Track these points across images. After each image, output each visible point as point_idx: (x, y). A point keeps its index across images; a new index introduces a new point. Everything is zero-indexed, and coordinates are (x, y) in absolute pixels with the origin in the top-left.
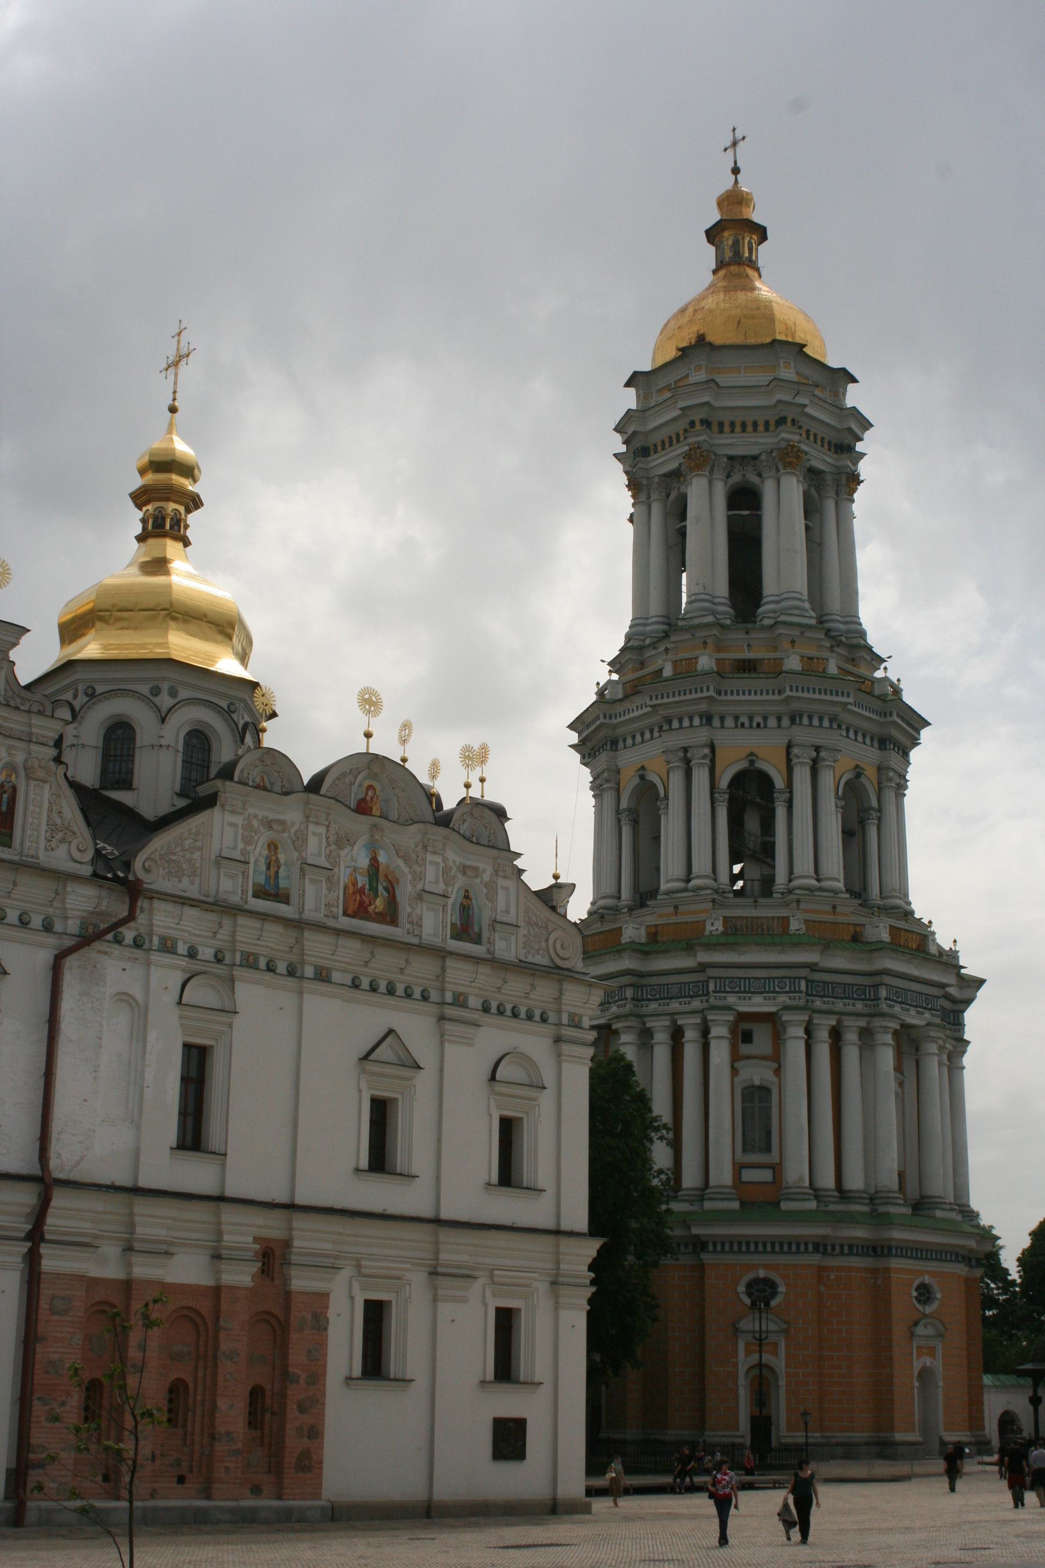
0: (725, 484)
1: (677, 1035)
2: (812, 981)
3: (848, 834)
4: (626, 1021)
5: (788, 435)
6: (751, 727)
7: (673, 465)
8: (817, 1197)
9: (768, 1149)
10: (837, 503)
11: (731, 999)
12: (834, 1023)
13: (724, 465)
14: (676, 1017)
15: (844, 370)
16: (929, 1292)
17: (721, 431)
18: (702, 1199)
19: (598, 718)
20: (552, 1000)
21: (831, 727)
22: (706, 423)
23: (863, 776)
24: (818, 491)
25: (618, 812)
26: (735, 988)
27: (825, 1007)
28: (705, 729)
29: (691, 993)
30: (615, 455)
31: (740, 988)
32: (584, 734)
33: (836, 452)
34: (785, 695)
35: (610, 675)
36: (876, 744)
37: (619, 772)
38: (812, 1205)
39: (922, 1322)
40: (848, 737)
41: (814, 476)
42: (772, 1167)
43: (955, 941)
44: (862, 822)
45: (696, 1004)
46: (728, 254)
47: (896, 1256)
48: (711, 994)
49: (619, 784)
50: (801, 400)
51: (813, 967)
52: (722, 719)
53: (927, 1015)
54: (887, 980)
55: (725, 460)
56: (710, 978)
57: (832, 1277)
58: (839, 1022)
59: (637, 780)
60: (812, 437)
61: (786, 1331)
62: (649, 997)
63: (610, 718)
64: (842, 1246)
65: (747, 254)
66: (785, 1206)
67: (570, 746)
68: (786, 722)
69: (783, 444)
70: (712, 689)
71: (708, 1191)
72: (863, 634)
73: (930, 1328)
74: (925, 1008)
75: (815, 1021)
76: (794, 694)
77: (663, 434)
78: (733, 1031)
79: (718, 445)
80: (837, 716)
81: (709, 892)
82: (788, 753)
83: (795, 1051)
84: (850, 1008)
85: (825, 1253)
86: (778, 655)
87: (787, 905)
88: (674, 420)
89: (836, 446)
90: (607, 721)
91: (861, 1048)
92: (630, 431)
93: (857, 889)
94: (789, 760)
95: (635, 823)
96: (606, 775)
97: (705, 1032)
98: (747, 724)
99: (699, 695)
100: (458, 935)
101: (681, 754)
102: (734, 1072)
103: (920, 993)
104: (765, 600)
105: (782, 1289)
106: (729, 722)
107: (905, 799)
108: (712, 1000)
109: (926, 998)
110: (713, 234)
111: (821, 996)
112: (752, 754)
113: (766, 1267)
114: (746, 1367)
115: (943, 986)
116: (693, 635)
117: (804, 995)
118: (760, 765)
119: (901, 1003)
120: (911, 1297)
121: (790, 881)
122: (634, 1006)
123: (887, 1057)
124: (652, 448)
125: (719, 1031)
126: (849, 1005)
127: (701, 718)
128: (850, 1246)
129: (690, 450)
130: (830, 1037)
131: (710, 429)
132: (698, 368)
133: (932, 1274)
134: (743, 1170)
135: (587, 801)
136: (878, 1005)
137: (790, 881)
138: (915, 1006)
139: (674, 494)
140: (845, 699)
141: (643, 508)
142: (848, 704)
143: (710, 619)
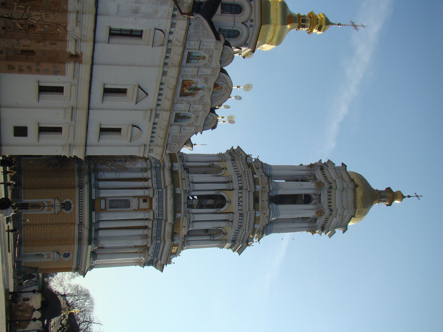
0: (312, 193)
1: (146, 180)
2: (162, 220)
3: (207, 231)
4: (150, 164)
5: (327, 212)
6: (239, 201)
7: (318, 177)
8: (96, 222)
9: (111, 207)
10: (306, 227)
11: (156, 196)
12: (149, 227)
13: (318, 193)
15: (346, 229)
16: (67, 257)
17: (328, 192)
18: (95, 188)
19: (241, 155)
20: (157, 144)
21: (239, 226)
22: (331, 188)
23: (224, 235)
24: (310, 221)
26: (160, 197)
27: (154, 224)
28: (238, 187)
30: (321, 160)
32: (236, 151)
33: (322, 227)
34: (248, 212)
35: (254, 159)
36: (234, 239)
37: (225, 161)
38: (94, 221)
39: (58, 255)
40: (236, 230)
41: (315, 220)
43: (174, 263)
45: (155, 185)
46: (383, 194)
48: (158, 190)
49: (221, 161)
50: (338, 216)
51: (166, 220)
52: (241, 193)
54: (162, 243)
56: (163, 189)
57: (72, 227)
59: (222, 167)
60: (326, 219)
61: (55, 213)
62: (157, 171)
65: (383, 200)
66: (94, 213)
67: (232, 146)
68: (240, 212)
69: (324, 211)
71: (98, 189)
72: (267, 234)
74: (154, 254)
75: (150, 221)
76: (249, 214)
77: (327, 175)
78: (147, 197)
79: (324, 191)
80: (242, 227)
81: (189, 189)
82: (230, 213)
83: (141, 215)
84: (154, 232)
85: (79, 225)
86: (260, 210)
87: (185, 213)
88: (332, 178)
89: (324, 227)
92: (328, 164)
93: (190, 233)
94: (229, 213)
95: (209, 167)
97: (146, 188)
98: (239, 200)
99: (248, 186)
100: (177, 115)
102: (134, 197)
103: (158, 253)
104: (276, 205)
105: (68, 212)
106: (240, 195)
107: (217, 248)
109: (157, 255)
110: (389, 189)
111: (157, 223)
112: (230, 202)
114: (43, 202)
115: (161, 259)
116: (266, 184)
117: (158, 218)
118: (227, 204)
119: (155, 247)
120: (66, 251)
121: (192, 213)
122: (154, 167)
123: (139, 243)
124: (323, 171)
125: (147, 193)
126: (155, 231)
127: (241, 186)
128: (81, 233)
129: (323, 183)
130: (145, 226)
131: (329, 189)
132: (348, 185)
133: (73, 257)
134: (104, 200)
135: (215, 152)
136: (155, 240)
137: (192, 213)
138: (154, 251)
139: (309, 178)
140: (247, 230)
141: (305, 168)
142: (246, 231)
143: (271, 189)
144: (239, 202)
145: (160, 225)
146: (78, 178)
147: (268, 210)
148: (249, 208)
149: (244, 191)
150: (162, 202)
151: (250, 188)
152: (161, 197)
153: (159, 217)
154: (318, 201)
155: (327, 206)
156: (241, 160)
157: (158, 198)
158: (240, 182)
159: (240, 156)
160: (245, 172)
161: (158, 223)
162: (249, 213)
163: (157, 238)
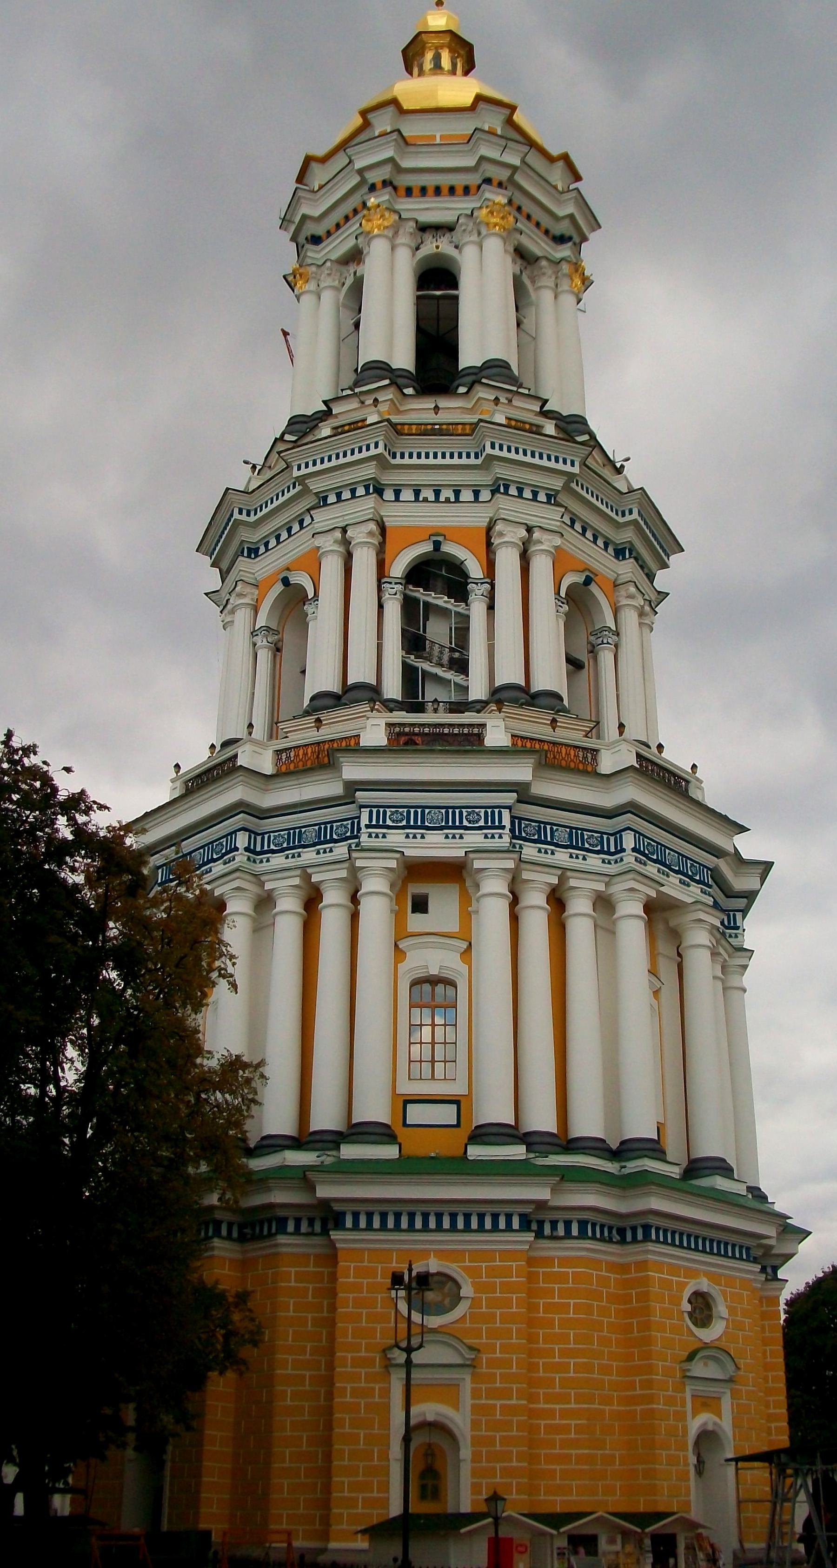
0: (414, 255)
3: (574, 664)
6: (437, 500)
7: (351, 243)
10: (556, 297)
11: (395, 838)
12: (555, 881)
13: (411, 230)
14: (309, 870)
23: (593, 583)
24: (533, 282)
25: (254, 633)
26: (401, 821)
29: (335, 837)
31: (408, 821)
34: (484, 455)
36: (610, 549)
39: (698, 1357)
42: (456, 1101)
44: (593, 651)
45: (341, 850)
47: (657, 1241)
48: (364, 830)
52: (397, 493)
53: (695, 889)
55: (412, 224)
56: (362, 807)
58: (562, 879)
61: (472, 1365)
62: (272, 847)
63: (248, 515)
64: (568, 1224)
67: (206, 594)
68: (485, 495)
70: (381, 445)
73: (711, 1364)
75: (525, 875)
76: (496, 452)
77: (337, 216)
78: (398, 890)
84: (578, 864)
85: (539, 1235)
90: (244, 517)
91: (595, 926)
92: (297, 219)
95: (277, 649)
96: (238, 588)
98: (431, 497)
99: (365, 454)
101: (338, 534)
102: (399, 954)
103: (683, 856)
105: (467, 1290)
106: (407, 495)
108: (364, 838)
109: (692, 865)
113: (442, 1254)
116: (363, 403)
117: (507, 831)
118: (449, 548)
122: (249, 859)
127: (367, 488)
134: (408, 1105)
136: (622, 860)
139: (349, 281)
144: (442, 499)
145: (545, 828)
146: (282, 1239)
147: (481, 395)
148: (468, 456)
149: (390, 478)
150: (427, 811)
151: (376, 446)
152: (402, 814)
153: (503, 827)
154: (448, 235)
155: (466, 198)
156: (252, 513)
157: (403, 828)
158: (346, 495)
159: (236, 515)
160: (301, 480)
161: (536, 837)
162: (488, 450)
163: (612, 849)
